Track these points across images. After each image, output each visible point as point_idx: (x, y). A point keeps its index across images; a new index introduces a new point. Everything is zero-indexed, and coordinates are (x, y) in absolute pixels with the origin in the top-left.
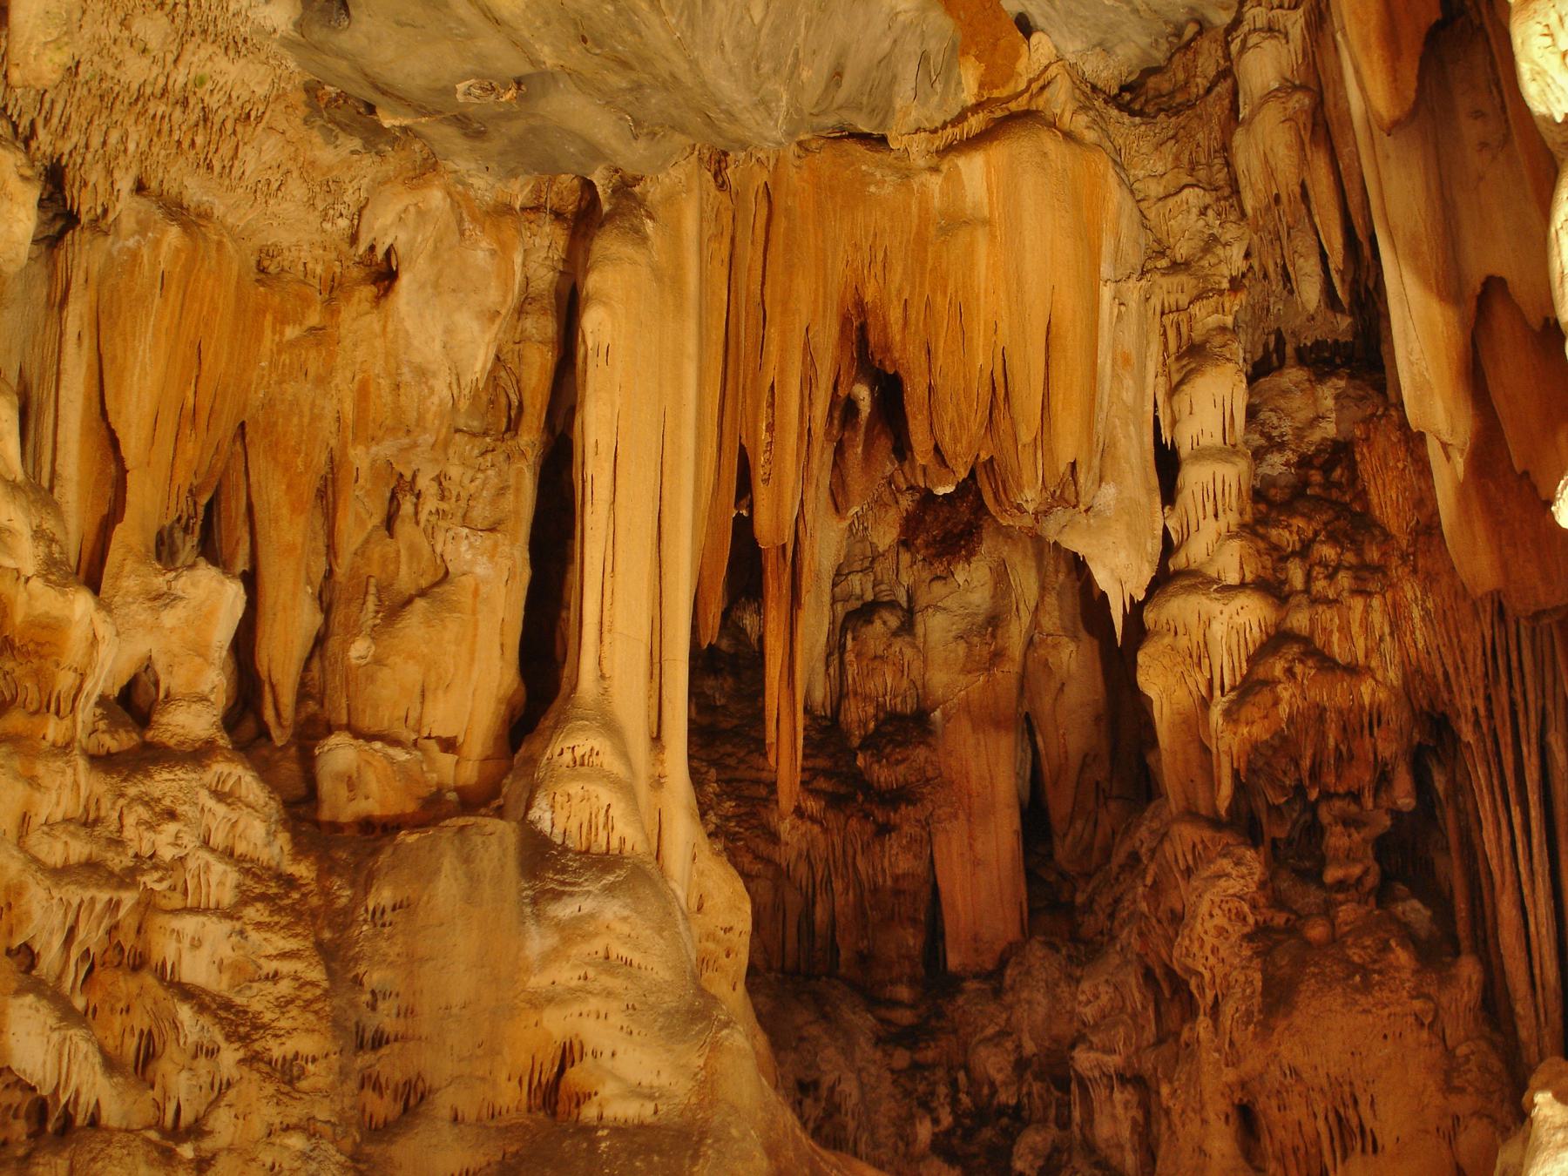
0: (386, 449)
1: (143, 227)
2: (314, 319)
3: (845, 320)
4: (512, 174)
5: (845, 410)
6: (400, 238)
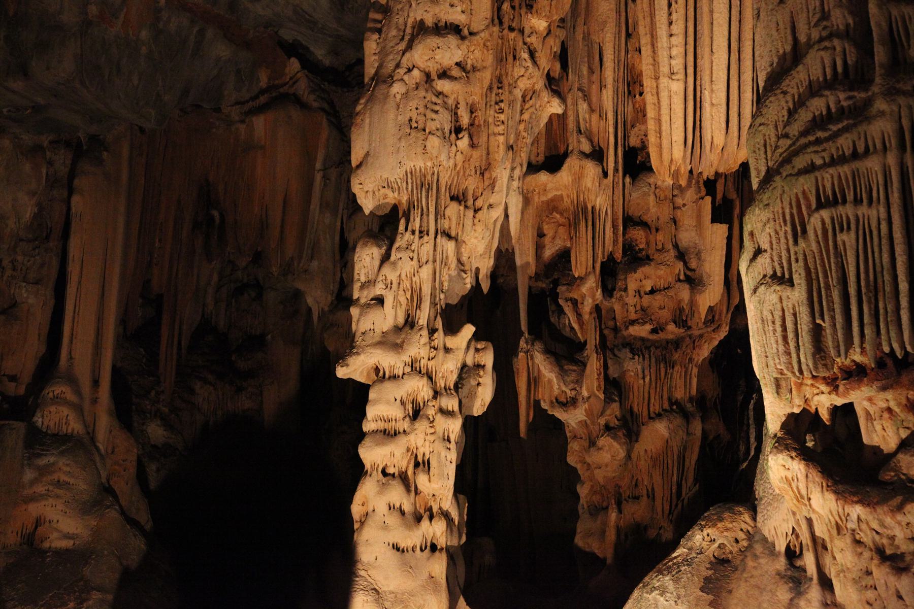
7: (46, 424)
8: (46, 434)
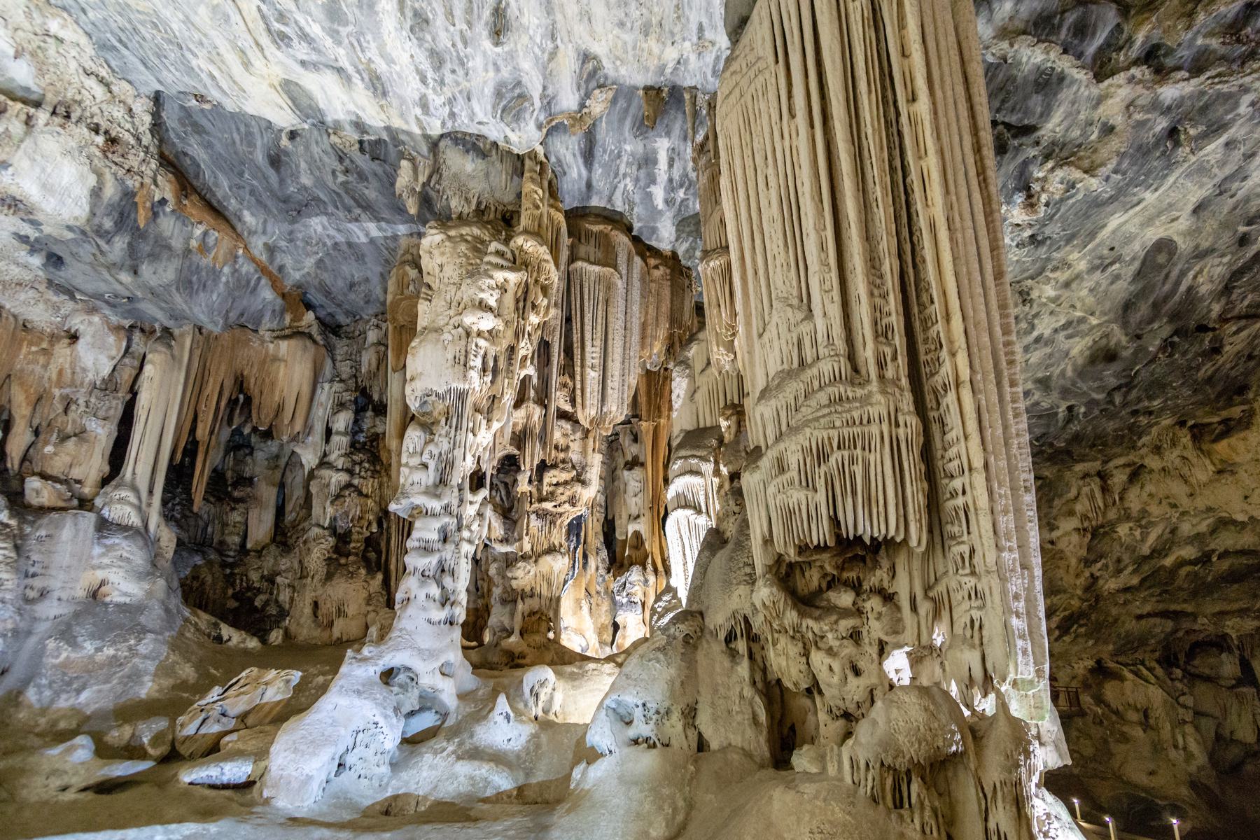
3: (236, 379)
5: (233, 403)
8: (112, 523)
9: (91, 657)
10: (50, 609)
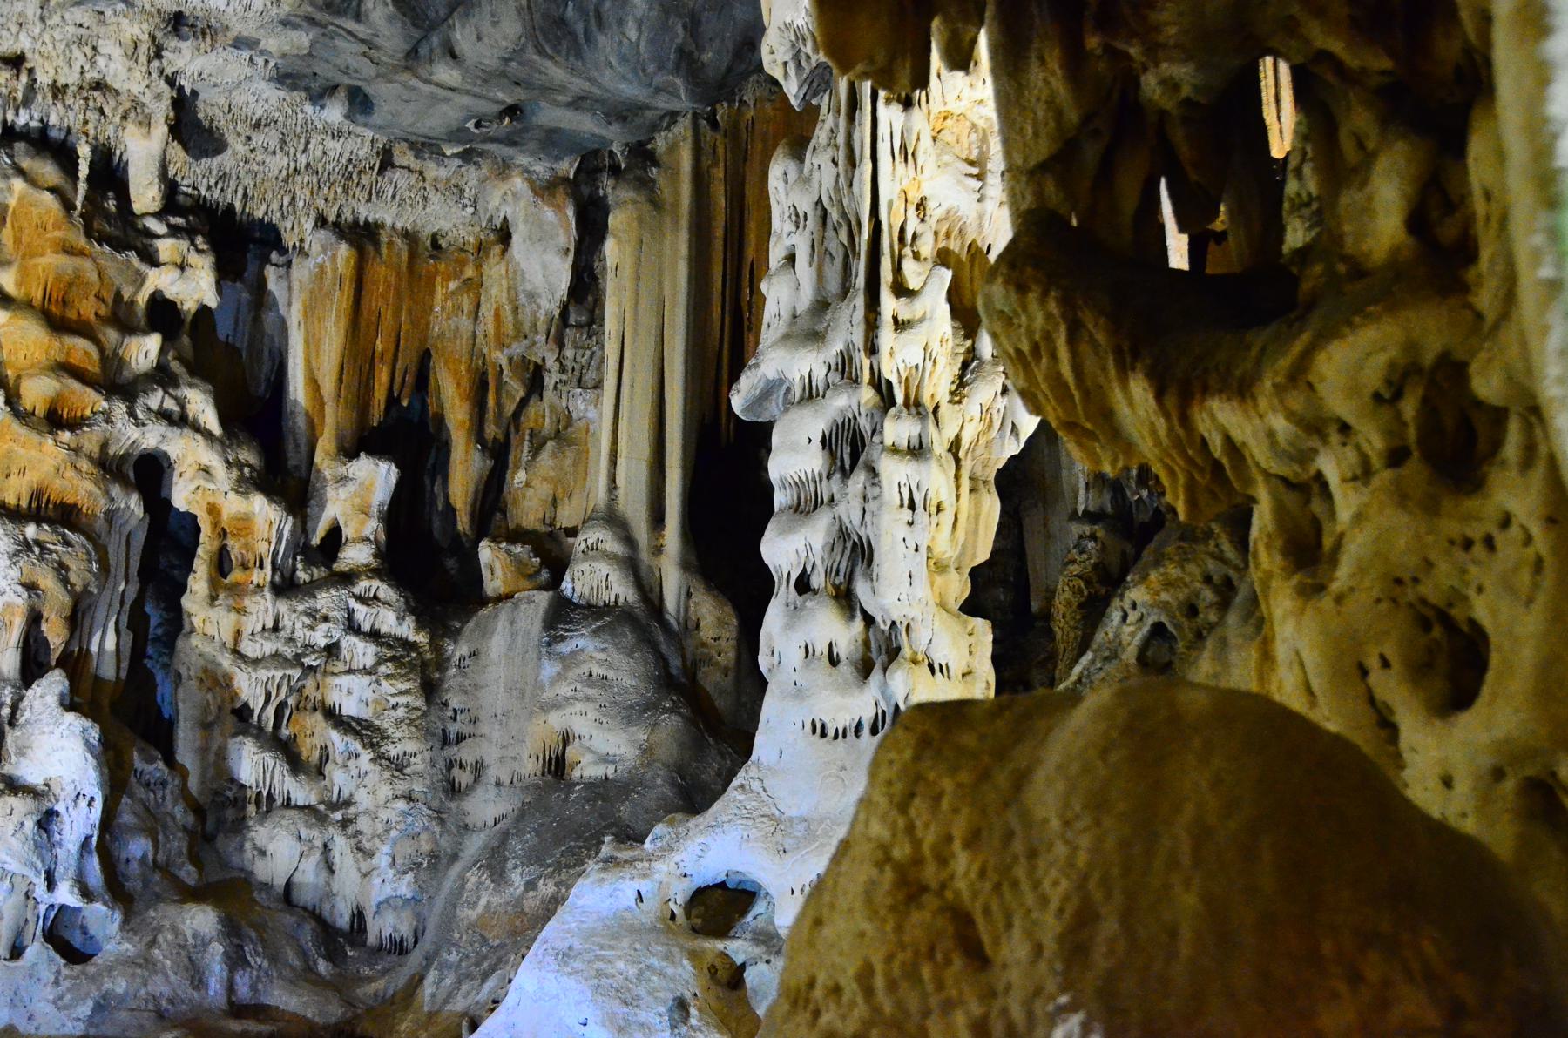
0: (517, 349)
1: (324, 250)
2: (469, 272)
4: (558, 158)
6: (507, 210)
7: (578, 590)
8: (577, 606)
9: (518, 902)
10: (487, 807)
